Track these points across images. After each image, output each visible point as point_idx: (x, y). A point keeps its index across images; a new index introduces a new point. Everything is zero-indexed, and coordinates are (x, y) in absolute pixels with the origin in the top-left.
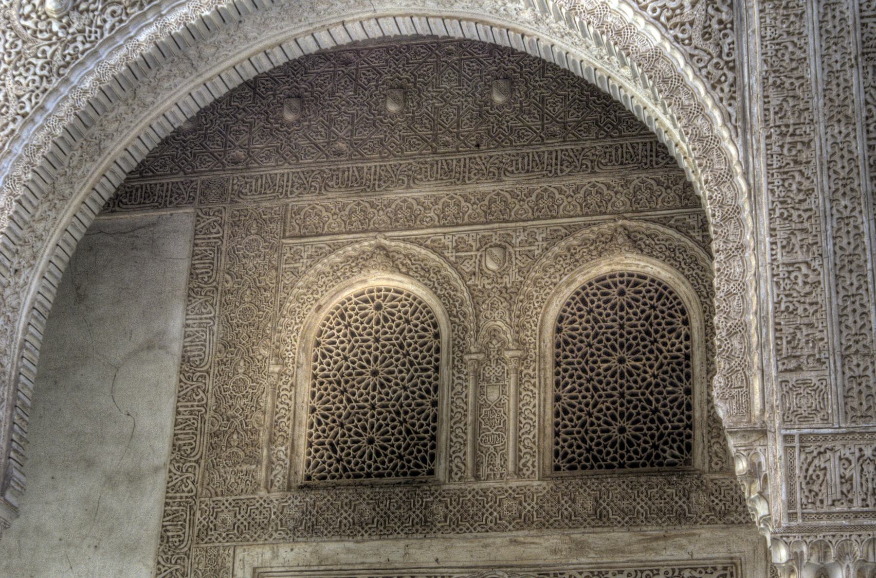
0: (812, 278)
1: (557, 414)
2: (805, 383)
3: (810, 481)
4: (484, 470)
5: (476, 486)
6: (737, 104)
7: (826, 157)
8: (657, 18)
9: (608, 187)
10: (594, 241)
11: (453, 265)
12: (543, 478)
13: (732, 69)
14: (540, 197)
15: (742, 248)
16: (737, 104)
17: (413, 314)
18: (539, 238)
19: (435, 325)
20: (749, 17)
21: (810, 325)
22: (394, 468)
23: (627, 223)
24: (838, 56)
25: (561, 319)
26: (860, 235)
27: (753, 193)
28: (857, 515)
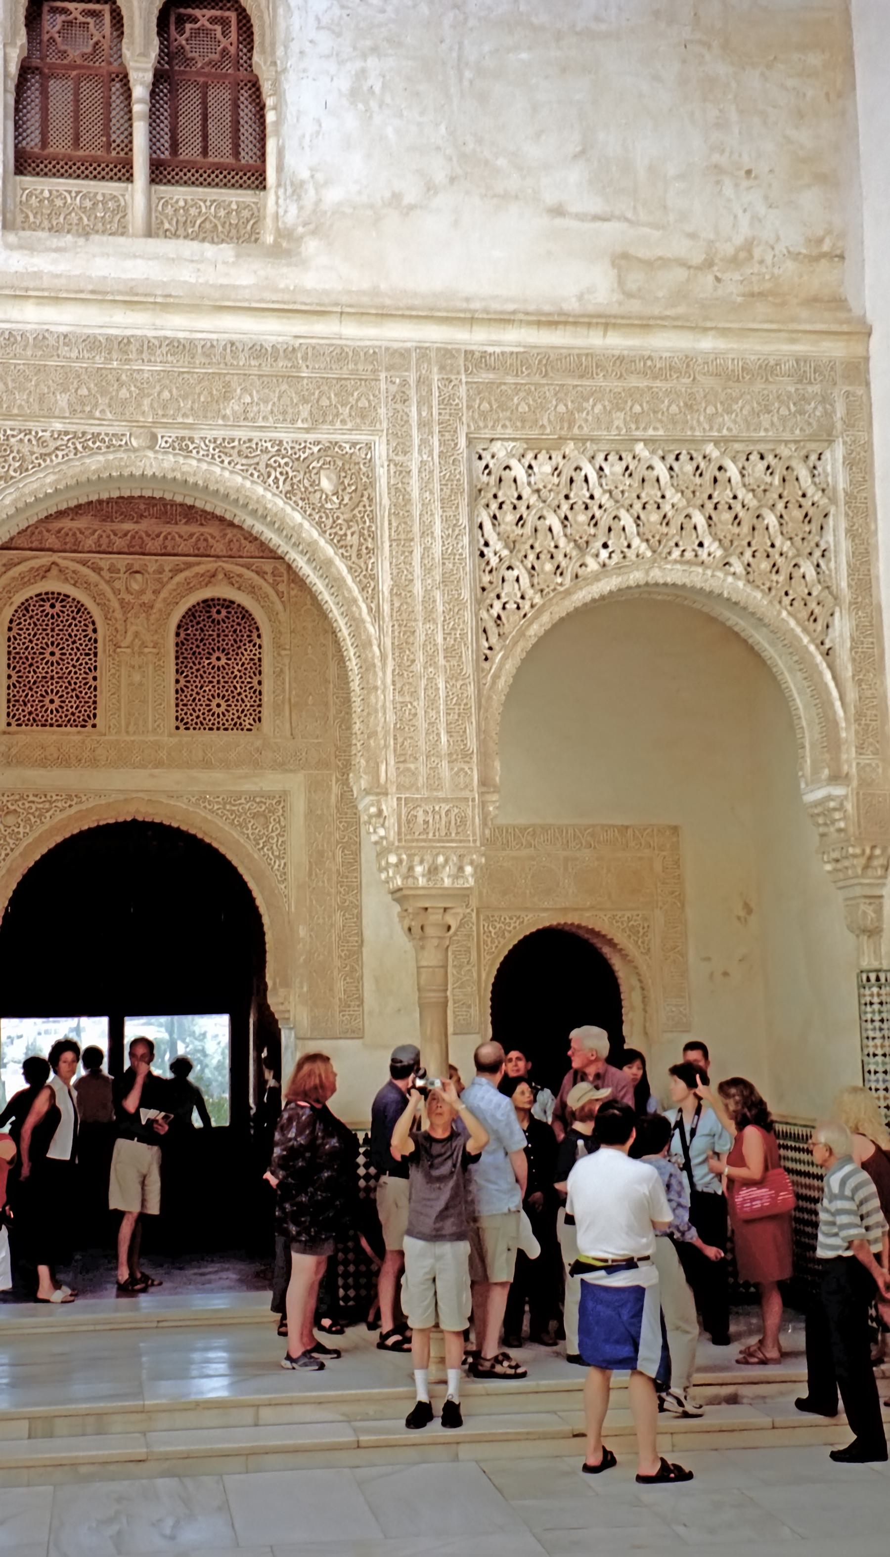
0: (413, 711)
1: (177, 692)
2: (408, 769)
3: (408, 822)
4: (132, 728)
5: (128, 738)
6: (375, 601)
7: (422, 642)
8: (332, 540)
9: (213, 537)
10: (202, 575)
11: (108, 582)
12: (171, 735)
13: (373, 579)
14: (166, 538)
15: (376, 688)
16: (375, 601)
17: (78, 613)
18: (167, 569)
19: (93, 623)
20: (383, 549)
21: (411, 738)
22: (69, 721)
23: (224, 565)
24: (429, 581)
25: (179, 627)
26: (437, 689)
27: (383, 657)
28: (430, 840)
